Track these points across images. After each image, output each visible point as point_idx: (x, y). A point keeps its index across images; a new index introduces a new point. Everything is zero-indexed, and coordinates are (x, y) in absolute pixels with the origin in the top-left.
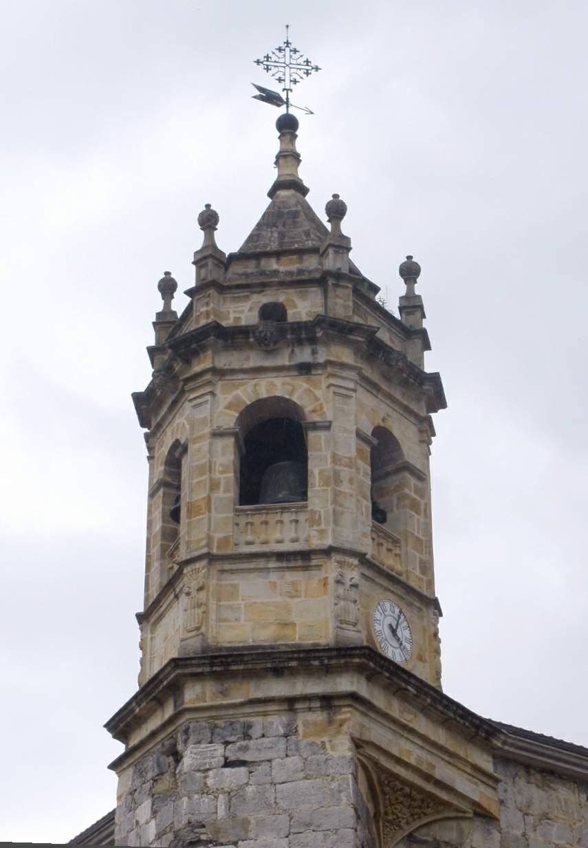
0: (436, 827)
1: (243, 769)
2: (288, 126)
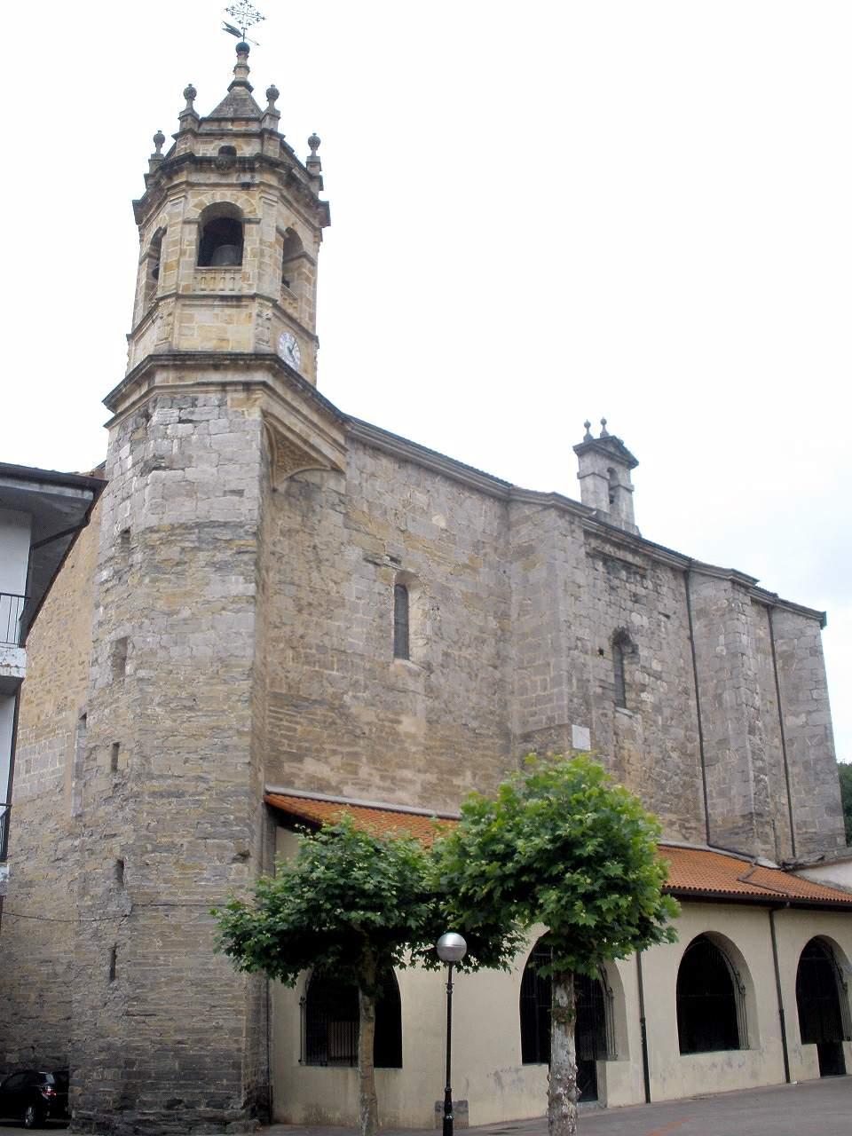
0: (307, 473)
1: (190, 425)
2: (243, 50)
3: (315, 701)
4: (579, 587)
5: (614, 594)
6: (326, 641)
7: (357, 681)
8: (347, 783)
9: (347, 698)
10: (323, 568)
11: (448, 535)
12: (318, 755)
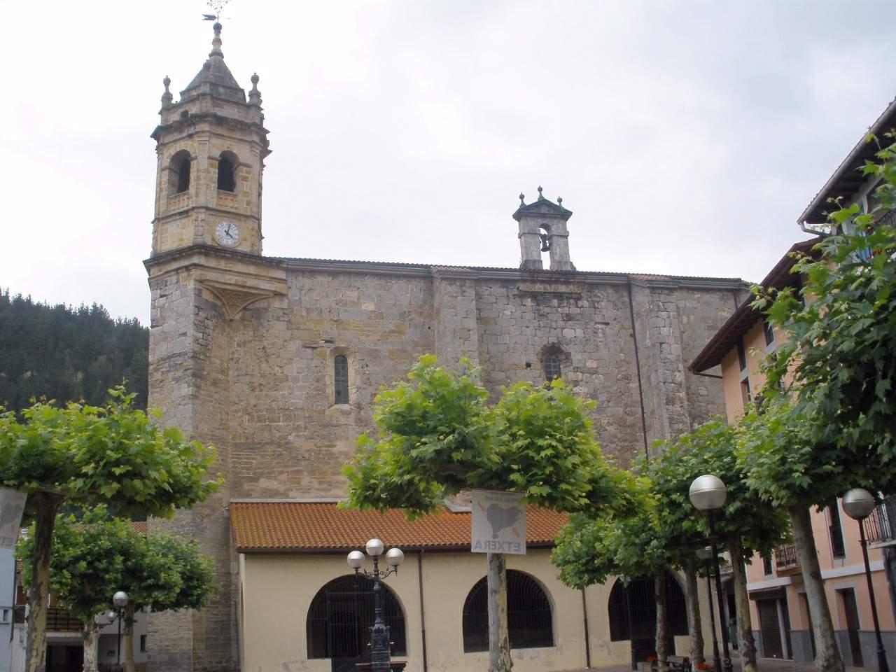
0: (257, 303)
1: (165, 298)
2: (218, 28)
3: (267, 443)
4: (469, 331)
5: (544, 319)
6: (274, 405)
7: (298, 426)
8: (292, 490)
9: (291, 438)
10: (270, 360)
11: (378, 315)
12: (269, 476)
